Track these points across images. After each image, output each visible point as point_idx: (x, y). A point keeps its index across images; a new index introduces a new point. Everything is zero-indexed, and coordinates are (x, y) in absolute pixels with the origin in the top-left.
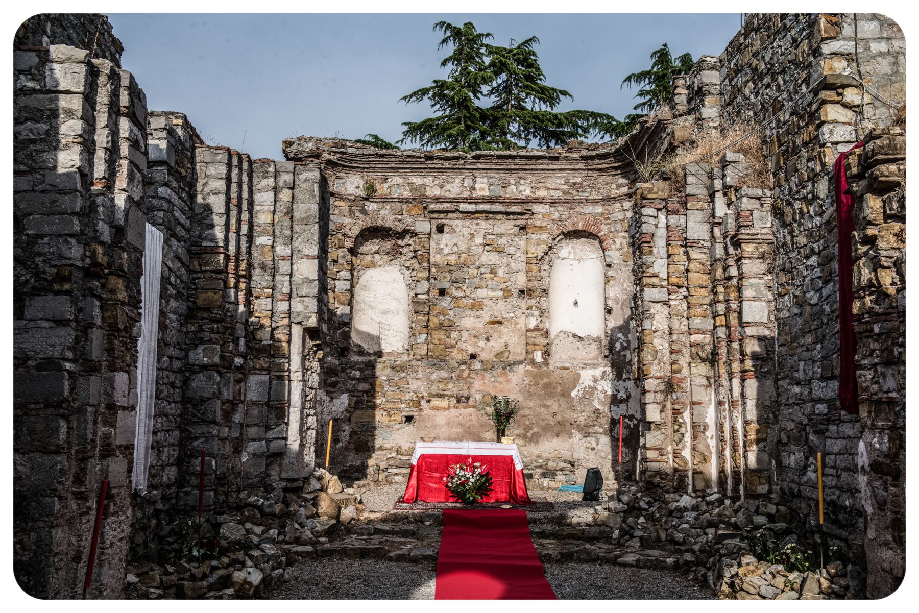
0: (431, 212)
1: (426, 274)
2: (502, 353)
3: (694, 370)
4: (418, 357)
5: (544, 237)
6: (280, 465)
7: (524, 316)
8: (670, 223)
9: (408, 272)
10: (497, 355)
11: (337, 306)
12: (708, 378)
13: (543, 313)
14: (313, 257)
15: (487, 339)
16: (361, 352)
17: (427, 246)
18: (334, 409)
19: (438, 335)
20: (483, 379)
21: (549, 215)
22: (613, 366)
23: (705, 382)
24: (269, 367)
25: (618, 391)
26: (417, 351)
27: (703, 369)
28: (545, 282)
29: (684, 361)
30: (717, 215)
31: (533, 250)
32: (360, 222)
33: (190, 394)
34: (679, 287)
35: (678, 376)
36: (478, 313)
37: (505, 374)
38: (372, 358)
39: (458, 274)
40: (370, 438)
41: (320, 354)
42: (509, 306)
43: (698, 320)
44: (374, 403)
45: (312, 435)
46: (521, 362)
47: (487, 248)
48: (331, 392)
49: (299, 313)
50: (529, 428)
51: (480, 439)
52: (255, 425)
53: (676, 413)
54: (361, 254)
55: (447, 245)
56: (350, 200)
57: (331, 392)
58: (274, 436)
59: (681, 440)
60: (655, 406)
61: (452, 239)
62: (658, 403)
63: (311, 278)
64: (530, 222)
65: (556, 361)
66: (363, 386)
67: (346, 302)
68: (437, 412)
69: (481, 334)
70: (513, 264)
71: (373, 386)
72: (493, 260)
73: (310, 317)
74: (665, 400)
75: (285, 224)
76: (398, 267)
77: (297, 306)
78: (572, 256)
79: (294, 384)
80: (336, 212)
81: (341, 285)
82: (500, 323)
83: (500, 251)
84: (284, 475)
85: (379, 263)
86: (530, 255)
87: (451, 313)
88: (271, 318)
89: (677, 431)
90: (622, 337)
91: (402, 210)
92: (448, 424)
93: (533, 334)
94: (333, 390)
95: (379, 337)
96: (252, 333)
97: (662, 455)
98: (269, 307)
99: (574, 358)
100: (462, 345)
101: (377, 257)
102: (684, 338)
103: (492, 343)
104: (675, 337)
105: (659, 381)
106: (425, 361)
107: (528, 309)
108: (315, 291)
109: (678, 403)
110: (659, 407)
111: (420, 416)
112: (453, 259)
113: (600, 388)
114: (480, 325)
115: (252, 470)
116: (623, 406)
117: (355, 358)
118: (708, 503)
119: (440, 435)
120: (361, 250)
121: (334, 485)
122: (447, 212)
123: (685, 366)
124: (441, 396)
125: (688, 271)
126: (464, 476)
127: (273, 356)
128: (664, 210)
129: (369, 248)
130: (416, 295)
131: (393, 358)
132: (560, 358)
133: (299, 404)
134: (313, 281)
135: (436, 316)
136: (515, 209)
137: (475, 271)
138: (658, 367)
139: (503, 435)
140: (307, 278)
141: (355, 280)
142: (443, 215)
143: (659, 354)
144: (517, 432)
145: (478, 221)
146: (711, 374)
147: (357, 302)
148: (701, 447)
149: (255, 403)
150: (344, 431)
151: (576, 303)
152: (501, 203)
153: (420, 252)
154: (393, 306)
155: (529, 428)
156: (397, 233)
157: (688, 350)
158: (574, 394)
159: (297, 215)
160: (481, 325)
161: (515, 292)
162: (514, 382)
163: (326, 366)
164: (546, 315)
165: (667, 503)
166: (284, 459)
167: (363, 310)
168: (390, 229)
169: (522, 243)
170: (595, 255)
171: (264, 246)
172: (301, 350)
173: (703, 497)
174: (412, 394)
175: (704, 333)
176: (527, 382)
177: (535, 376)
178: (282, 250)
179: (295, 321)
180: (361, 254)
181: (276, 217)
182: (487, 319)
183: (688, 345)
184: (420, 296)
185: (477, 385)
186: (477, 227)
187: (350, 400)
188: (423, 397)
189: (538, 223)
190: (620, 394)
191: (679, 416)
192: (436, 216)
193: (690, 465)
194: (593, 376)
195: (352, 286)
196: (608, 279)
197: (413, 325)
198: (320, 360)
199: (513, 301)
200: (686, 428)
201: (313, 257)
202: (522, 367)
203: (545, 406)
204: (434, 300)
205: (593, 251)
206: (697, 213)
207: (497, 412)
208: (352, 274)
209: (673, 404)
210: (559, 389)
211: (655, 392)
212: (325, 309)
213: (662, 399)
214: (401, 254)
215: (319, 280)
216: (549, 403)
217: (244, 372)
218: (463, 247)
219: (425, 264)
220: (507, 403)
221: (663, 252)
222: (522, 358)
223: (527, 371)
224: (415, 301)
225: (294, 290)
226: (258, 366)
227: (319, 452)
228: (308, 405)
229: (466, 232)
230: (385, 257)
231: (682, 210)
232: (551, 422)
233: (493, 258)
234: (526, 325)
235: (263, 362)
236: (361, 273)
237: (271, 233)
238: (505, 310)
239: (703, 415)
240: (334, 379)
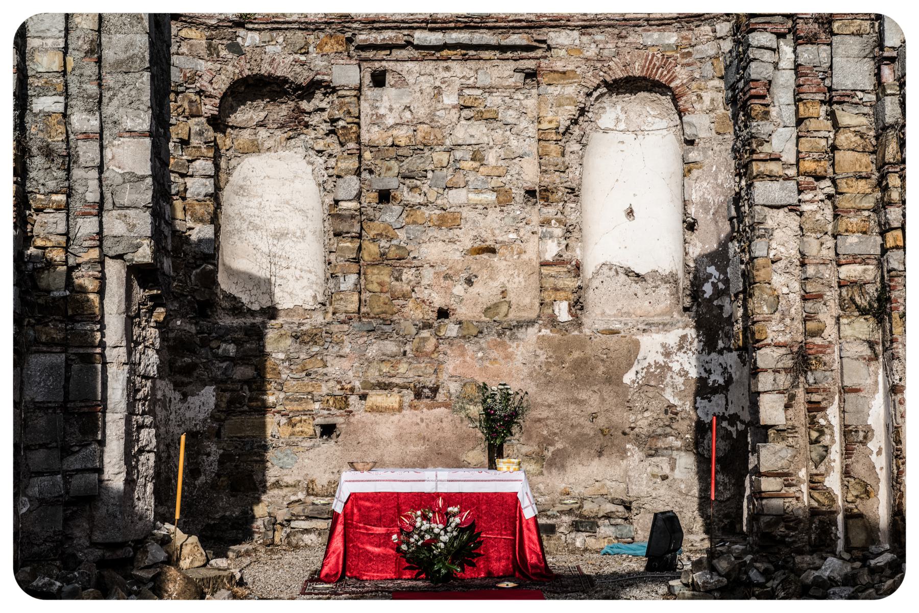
0: (362, 48)
1: (353, 164)
2: (496, 305)
3: (847, 331)
4: (343, 317)
5: (570, 90)
6: (91, 519)
7: (535, 238)
8: (801, 60)
9: (320, 160)
10: (487, 311)
11: (190, 224)
12: (871, 344)
13: (570, 231)
14: (142, 134)
15: (469, 282)
16: (237, 308)
17: (354, 110)
18: (188, 414)
19: (379, 276)
20: (462, 355)
21: (580, 49)
22: (698, 327)
23: (867, 352)
24: (66, 338)
25: (709, 372)
26: (341, 306)
27: (862, 328)
28: (573, 175)
29: (827, 314)
30: (888, 43)
31: (550, 116)
32: (230, 68)
34: (819, 178)
35: (818, 341)
36: (451, 234)
37: (503, 344)
38: (258, 320)
39: (413, 163)
40: (256, 467)
41: (160, 313)
42: (508, 220)
43: (853, 239)
44: (264, 401)
45: (148, 462)
46: (531, 323)
47: (465, 113)
48: (183, 384)
49: (118, 238)
50: (547, 442)
51: (458, 464)
52: (41, 446)
53: (815, 408)
54: (233, 127)
55: (391, 109)
56: (209, 27)
57: (183, 384)
58: (78, 466)
59: (823, 458)
60: (775, 396)
61: (400, 97)
62: (780, 392)
63: (140, 173)
64: (544, 63)
65: (594, 320)
66: (243, 372)
67: (208, 218)
68: (379, 417)
69: (457, 273)
70: (514, 143)
71: (261, 370)
72: (478, 135)
73: (138, 246)
74: (794, 385)
76: (301, 151)
77: (115, 225)
78: (622, 126)
79: (112, 370)
80: (184, 49)
81: (198, 187)
82: (492, 251)
83: (490, 118)
84: (98, 537)
85: (267, 145)
86: (545, 126)
87: (402, 234)
88: (66, 249)
89: (817, 441)
90: (716, 274)
91: (307, 44)
92: (399, 437)
93: (553, 270)
94: (186, 380)
95: (269, 281)
96: (31, 276)
97: (790, 485)
98: (62, 228)
99: (628, 314)
100: (424, 294)
101: (263, 133)
102: (827, 273)
103: (477, 288)
104: (811, 270)
105: (783, 351)
106: (355, 323)
107: (542, 224)
108: (148, 197)
109: (817, 391)
110: (784, 399)
111: (348, 423)
112: (402, 135)
113: (676, 367)
114: (454, 255)
115: (38, 529)
116: (719, 399)
117: (227, 321)
118: (873, 571)
119: (386, 458)
120: (233, 119)
121: (192, 553)
122: (390, 47)
123: (830, 322)
124: (385, 387)
125: (834, 148)
126: (430, 531)
127: (72, 320)
128: (790, 37)
129: (247, 116)
130: (337, 202)
131: (296, 320)
132: (603, 313)
133: (123, 406)
134: (143, 178)
135: (374, 240)
136: (516, 39)
137: (445, 157)
138: (781, 327)
139: (501, 455)
140: (132, 174)
141: (223, 176)
142: (382, 54)
143: (783, 301)
144: (525, 449)
145: (449, 63)
146: (878, 336)
147: (228, 217)
148: (859, 469)
150: (208, 455)
151: (630, 213)
152: (490, 28)
153: (341, 123)
154: (294, 223)
155: (547, 442)
156: (299, 87)
157: (835, 294)
158: (628, 378)
159: (109, 55)
160: (457, 256)
161: (519, 195)
162: (520, 358)
163: (172, 335)
164: (576, 234)
165: (798, 572)
167: (240, 231)
168: (285, 80)
169: (531, 103)
170: (664, 123)
171: (49, 115)
172: (123, 307)
173: (865, 560)
174: (332, 384)
175: (864, 262)
176: (543, 358)
177: (557, 348)
178: (82, 121)
179: (112, 253)
180: (233, 127)
181: (70, 59)
182: (468, 244)
183: (835, 284)
184: (344, 205)
185: (452, 365)
186: (447, 74)
187: (218, 397)
188: (352, 390)
189: (559, 66)
190: (713, 377)
191: (819, 415)
192: (370, 54)
193: (840, 503)
194: (663, 346)
195: (218, 188)
196: (688, 167)
197: (332, 257)
198: (159, 325)
199: (516, 210)
200: (832, 435)
201: (142, 134)
202: (532, 331)
203: (577, 402)
204: (370, 211)
205: (661, 116)
206: (851, 40)
207: (489, 413)
208: (217, 166)
209: (808, 392)
210: (601, 369)
211: (776, 371)
212: (167, 231)
213: (787, 384)
214: (307, 126)
215: (154, 176)
216: (583, 395)
218: (421, 112)
219: (352, 145)
220: (506, 397)
221: (788, 114)
222: (533, 315)
223: (542, 339)
224: (334, 212)
225: (108, 195)
226: (44, 338)
227: (163, 494)
228: (140, 408)
229: (426, 83)
230: (278, 132)
231: (823, 36)
232: (587, 430)
233: (478, 132)
234: (539, 254)
235: (54, 331)
236: (233, 162)
237: (61, 88)
238: (500, 228)
239: (862, 413)
240: (187, 360)
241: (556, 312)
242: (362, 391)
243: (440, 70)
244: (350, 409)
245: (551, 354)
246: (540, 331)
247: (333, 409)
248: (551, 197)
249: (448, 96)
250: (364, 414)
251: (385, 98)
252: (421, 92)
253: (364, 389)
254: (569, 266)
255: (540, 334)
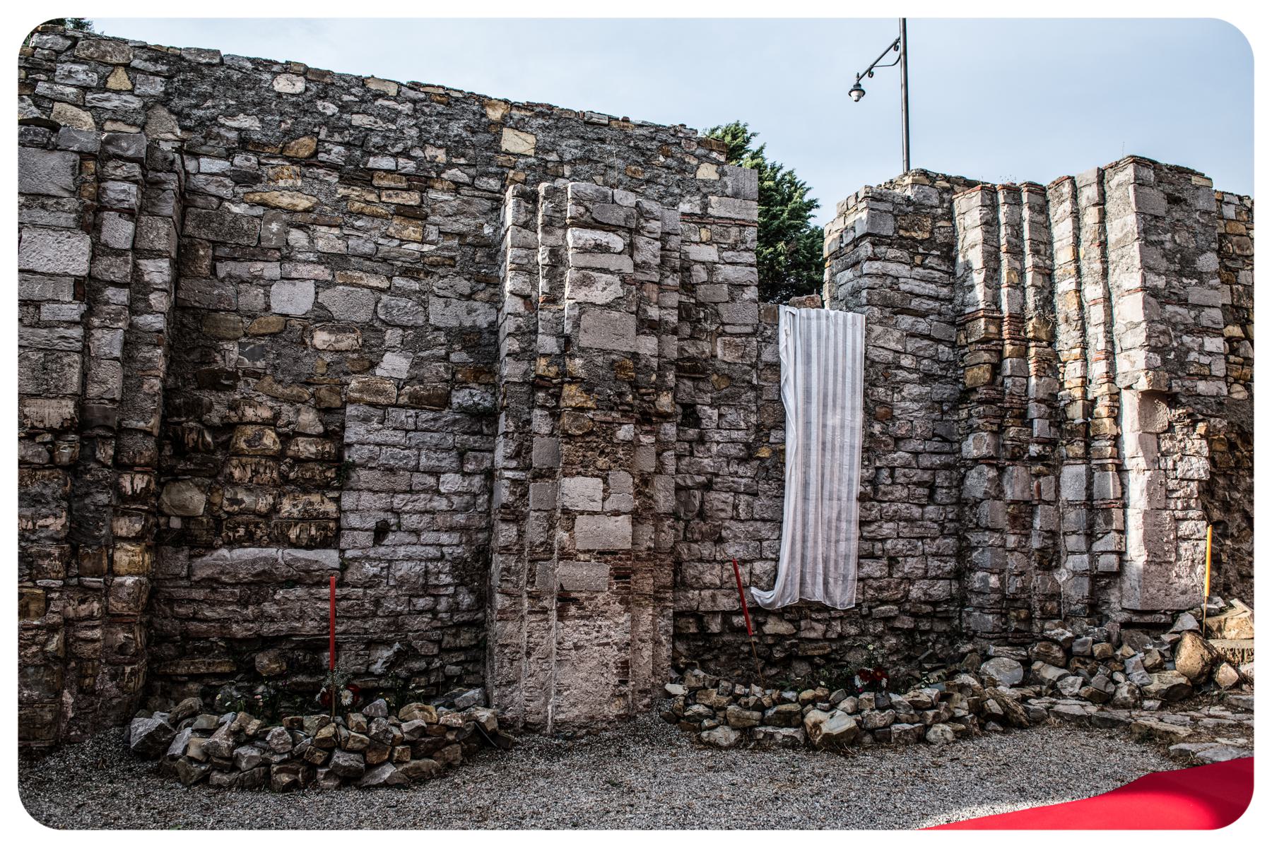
14: (1136, 291)
33: (965, 495)
75: (1093, 255)
84: (1126, 604)
140: (1131, 322)
149: (1071, 504)
166: (1123, 581)
201: (1136, 291)
217: (1050, 464)
226: (1071, 454)
235: (1077, 449)
237: (1073, 272)
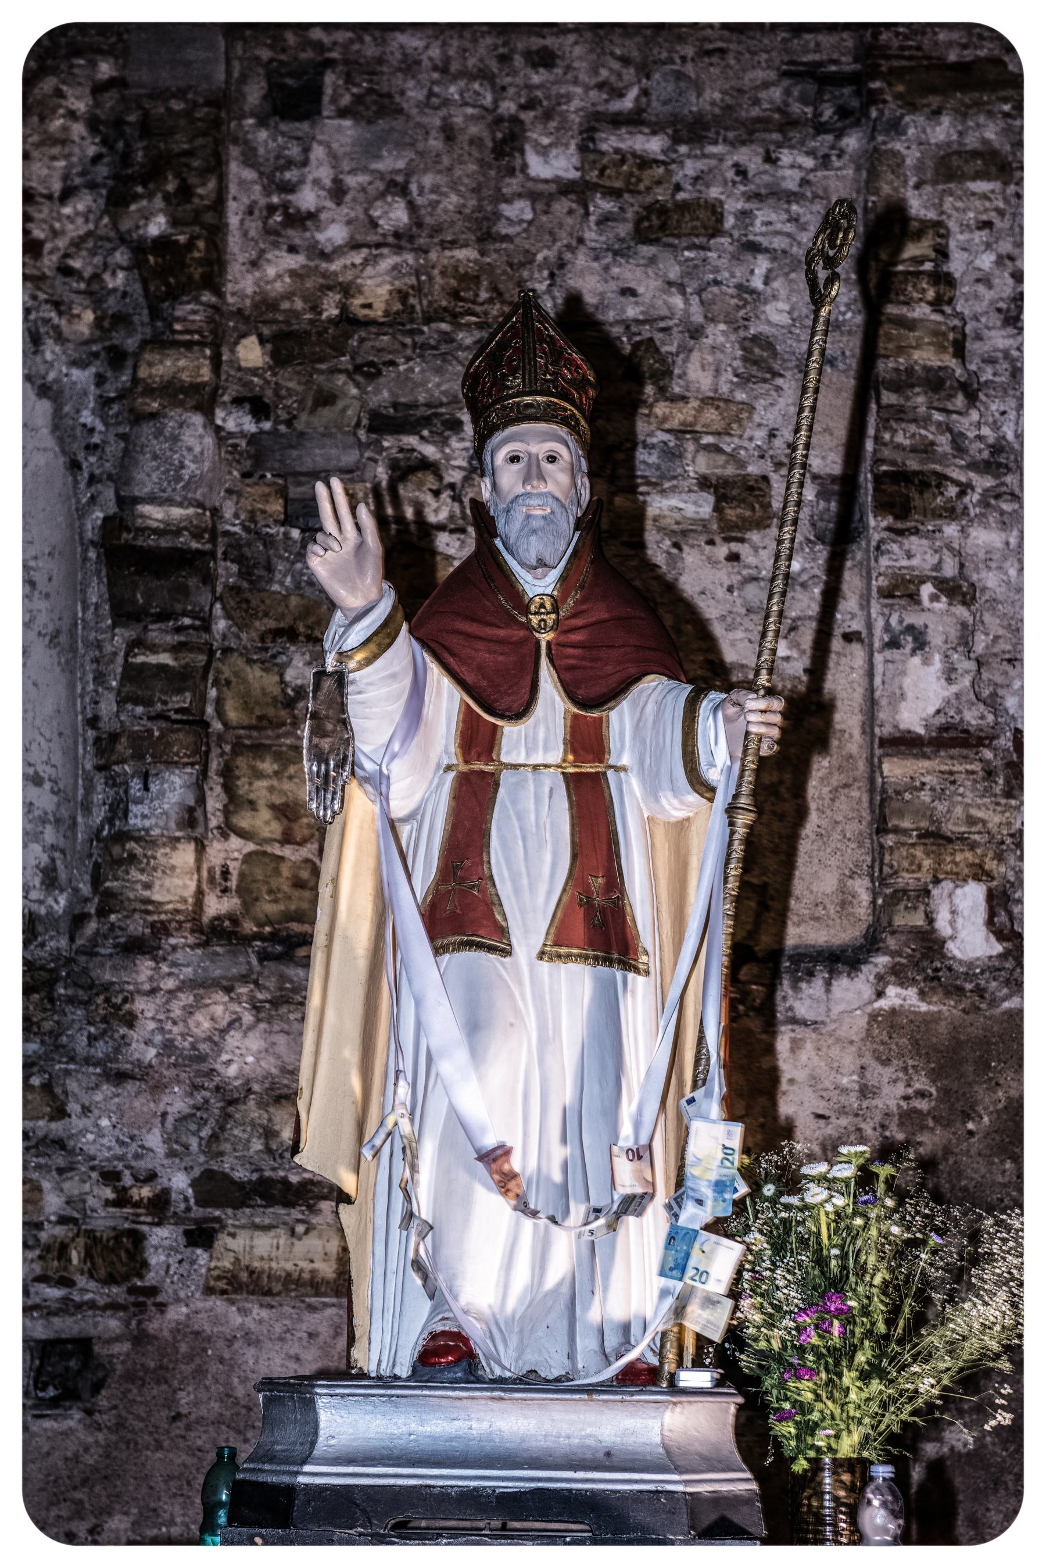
111: (140, 1339)
241: (942, 923)
242: (197, 1212)
243: (518, 61)
244: (151, 1278)
245: (921, 1083)
246: (880, 994)
247: (82, 1281)
248: (917, 501)
249: (543, 152)
250: (201, 1303)
251: (318, 152)
252: (449, 133)
253: (201, 1202)
254: (988, 754)
255: (883, 1004)
